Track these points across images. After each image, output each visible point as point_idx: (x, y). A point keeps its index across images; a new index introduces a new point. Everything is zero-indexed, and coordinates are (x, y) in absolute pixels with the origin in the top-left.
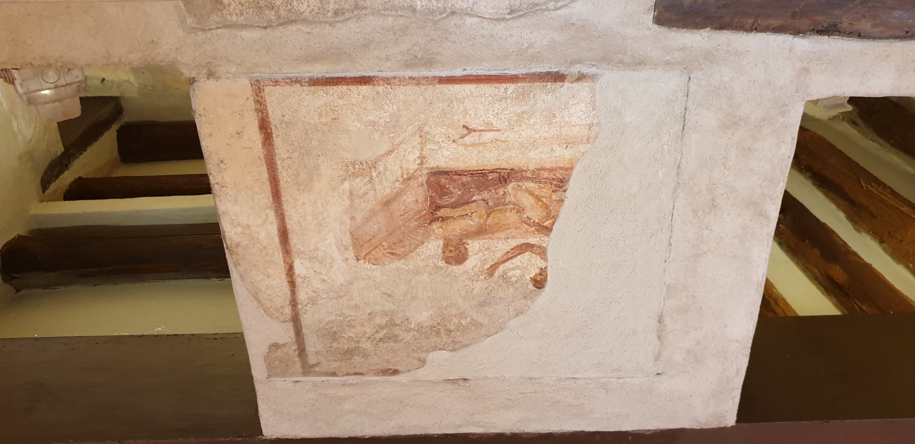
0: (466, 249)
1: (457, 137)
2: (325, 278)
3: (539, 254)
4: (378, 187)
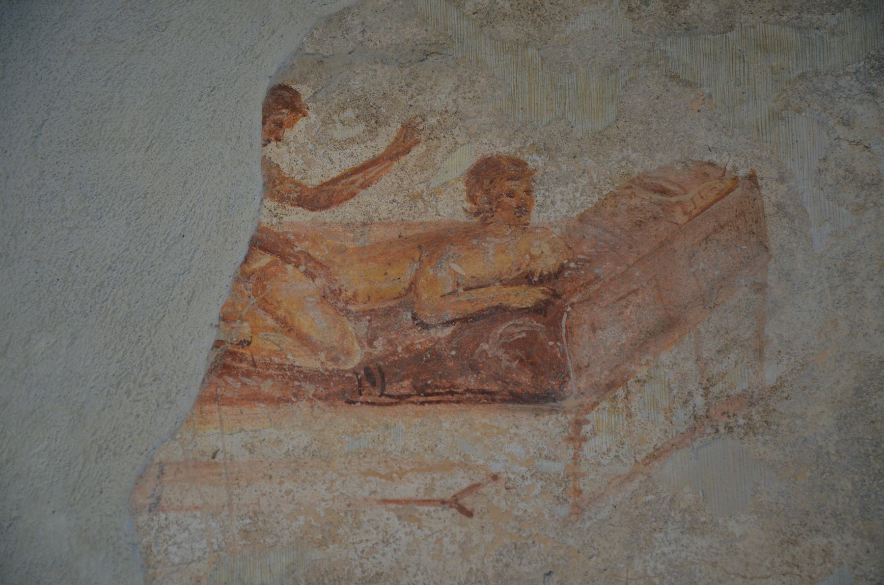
0: (472, 198)
1: (489, 489)
2: (841, 131)
3: (283, 180)
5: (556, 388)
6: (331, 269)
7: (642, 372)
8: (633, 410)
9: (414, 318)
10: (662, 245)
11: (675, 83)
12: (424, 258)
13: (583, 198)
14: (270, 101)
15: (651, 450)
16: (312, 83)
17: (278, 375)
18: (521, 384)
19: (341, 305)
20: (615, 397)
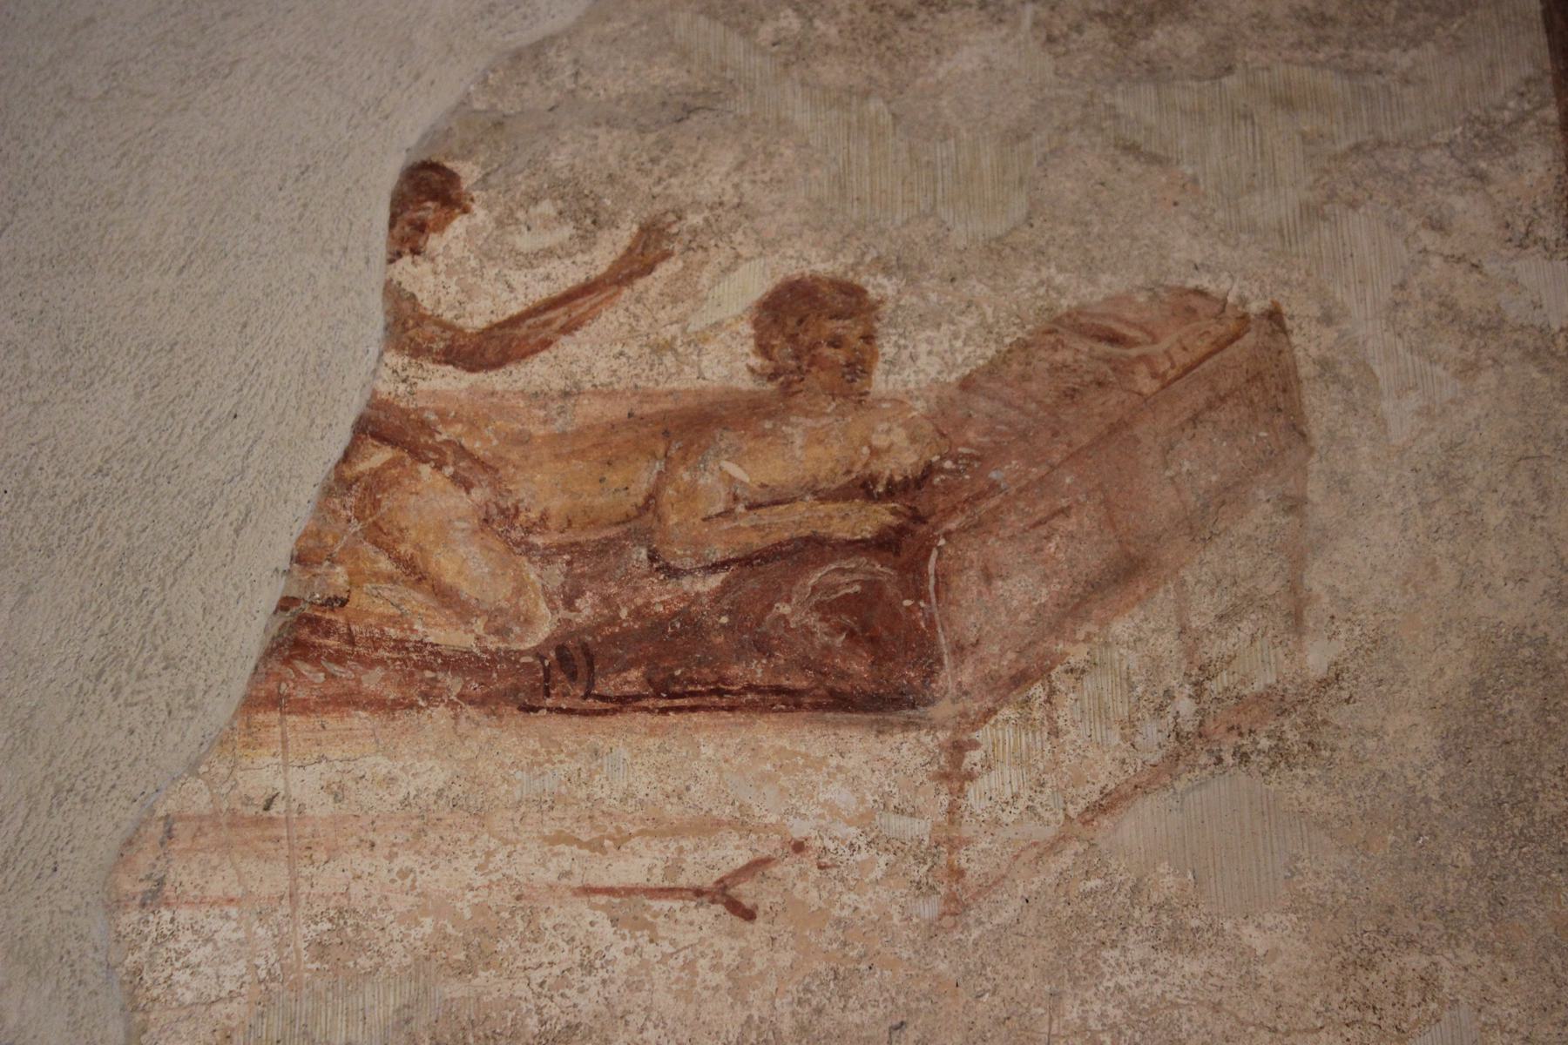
0: (764, 349)
1: (787, 868)
2: (1428, 238)
3: (421, 319)
4: (1167, 644)
5: (917, 683)
6: (502, 472)
7: (1078, 655)
8: (1061, 723)
9: (652, 558)
10: (1113, 429)
11: (1131, 158)
12: (673, 452)
13: (967, 350)
14: (406, 188)
15: (1096, 797)
16: (482, 159)
17: (394, 660)
18: (850, 676)
19: (516, 535)
20: (1027, 701)
